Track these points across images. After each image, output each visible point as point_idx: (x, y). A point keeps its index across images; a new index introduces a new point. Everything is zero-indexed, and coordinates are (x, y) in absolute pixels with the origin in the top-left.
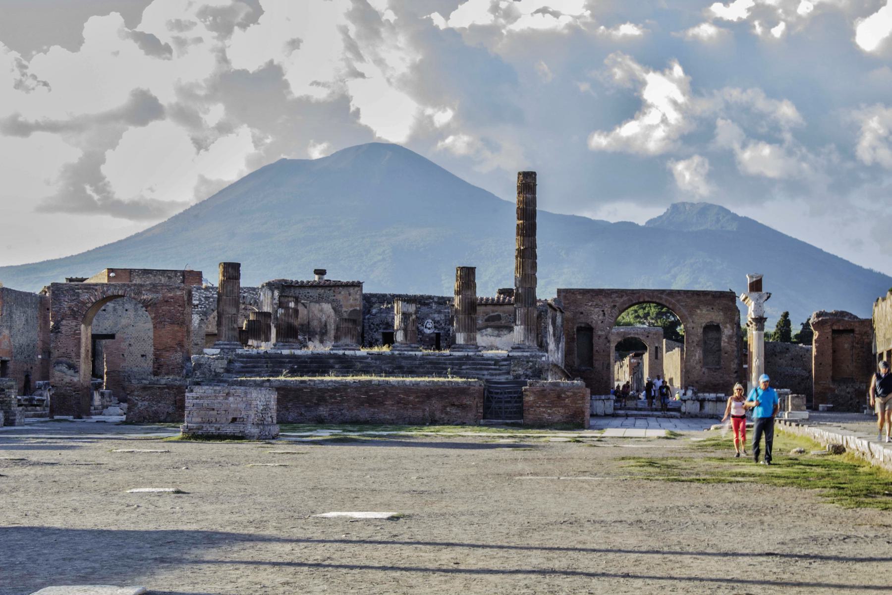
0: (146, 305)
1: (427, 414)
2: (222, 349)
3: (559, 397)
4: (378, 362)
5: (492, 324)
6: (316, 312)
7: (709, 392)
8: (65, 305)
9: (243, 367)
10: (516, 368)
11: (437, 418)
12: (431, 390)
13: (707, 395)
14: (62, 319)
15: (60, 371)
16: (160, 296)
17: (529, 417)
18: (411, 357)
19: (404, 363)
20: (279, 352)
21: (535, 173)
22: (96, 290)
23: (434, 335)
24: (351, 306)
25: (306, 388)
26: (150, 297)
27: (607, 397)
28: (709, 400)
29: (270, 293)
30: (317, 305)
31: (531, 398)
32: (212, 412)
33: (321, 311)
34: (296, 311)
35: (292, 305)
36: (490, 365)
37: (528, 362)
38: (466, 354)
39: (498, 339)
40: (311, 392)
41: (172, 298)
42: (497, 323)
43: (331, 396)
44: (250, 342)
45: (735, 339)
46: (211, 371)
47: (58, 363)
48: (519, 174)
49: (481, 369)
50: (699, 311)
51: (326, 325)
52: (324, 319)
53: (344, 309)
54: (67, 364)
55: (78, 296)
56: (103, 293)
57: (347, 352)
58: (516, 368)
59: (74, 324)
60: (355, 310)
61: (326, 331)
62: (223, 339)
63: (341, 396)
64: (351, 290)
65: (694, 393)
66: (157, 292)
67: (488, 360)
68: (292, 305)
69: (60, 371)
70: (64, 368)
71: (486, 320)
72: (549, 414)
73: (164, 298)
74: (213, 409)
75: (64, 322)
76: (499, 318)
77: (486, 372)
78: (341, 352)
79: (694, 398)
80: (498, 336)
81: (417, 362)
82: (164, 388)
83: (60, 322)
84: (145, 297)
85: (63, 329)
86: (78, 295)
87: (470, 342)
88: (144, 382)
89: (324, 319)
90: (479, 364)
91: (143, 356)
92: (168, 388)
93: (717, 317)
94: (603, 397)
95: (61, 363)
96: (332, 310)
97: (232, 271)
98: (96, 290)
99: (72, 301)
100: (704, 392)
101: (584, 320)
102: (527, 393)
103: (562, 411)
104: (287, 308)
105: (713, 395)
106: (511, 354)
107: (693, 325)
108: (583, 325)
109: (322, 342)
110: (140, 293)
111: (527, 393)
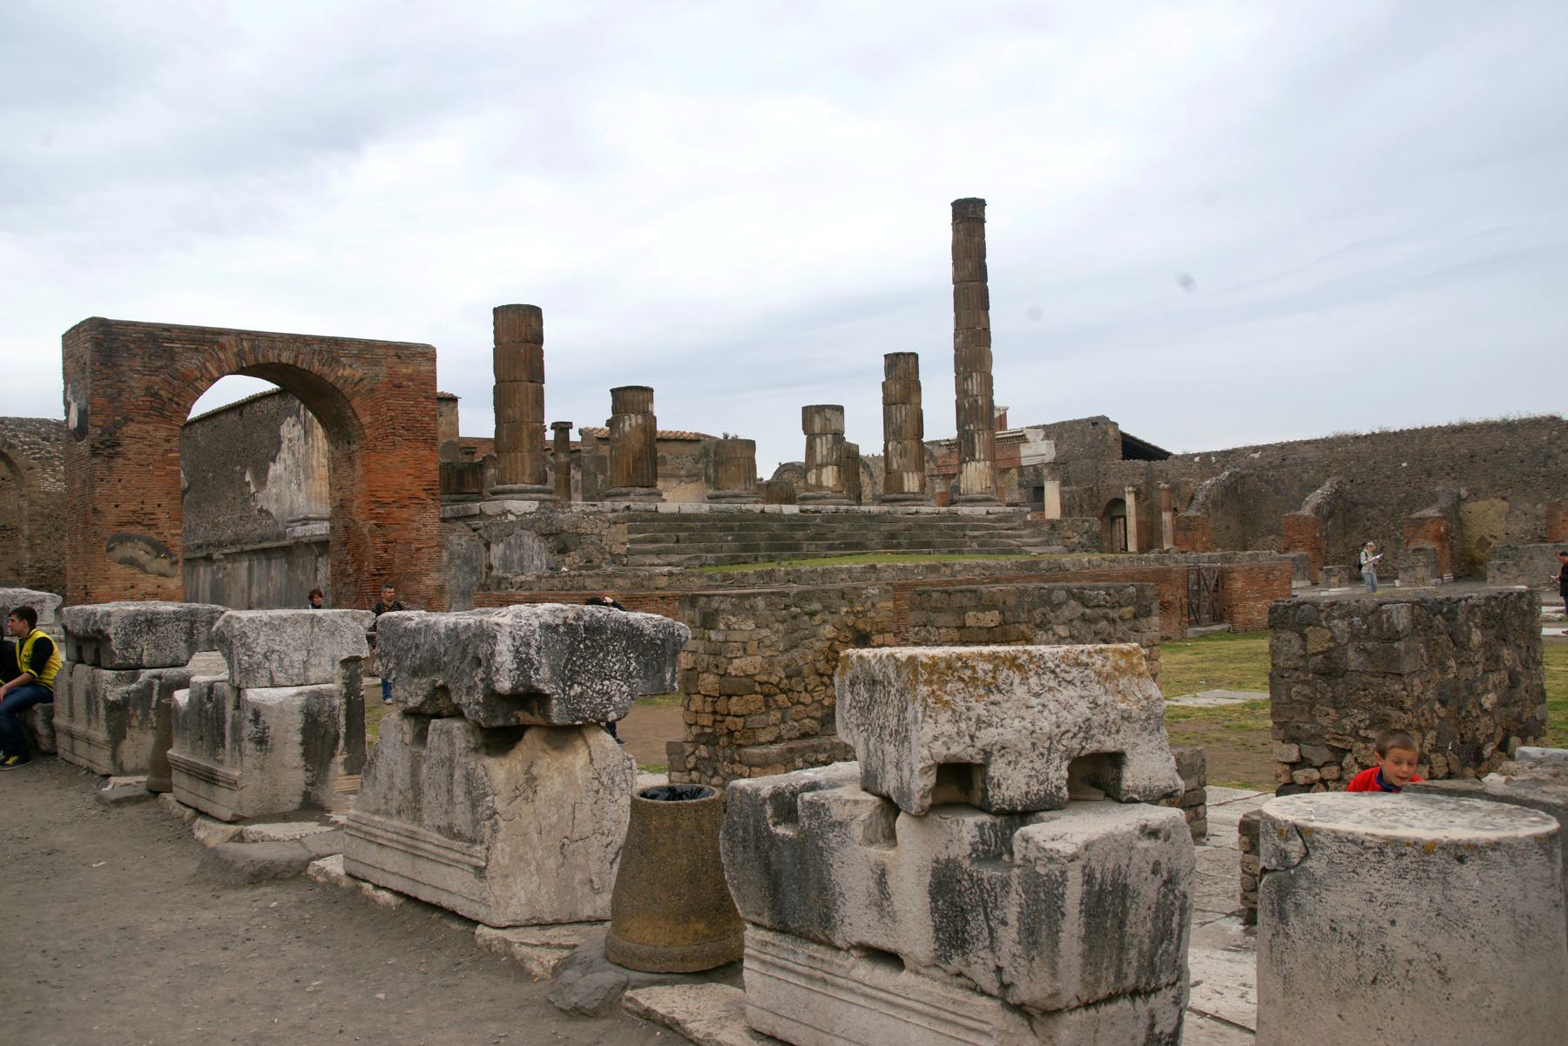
2: (542, 501)
3: (1267, 580)
10: (1069, 534)
14: (128, 420)
15: (131, 562)
16: (383, 371)
22: (222, 347)
26: (359, 374)
41: (410, 378)
46: (602, 551)
47: (123, 539)
54: (149, 542)
55: (172, 359)
59: (163, 434)
69: (131, 562)
70: (140, 552)
75: (132, 429)
83: (118, 426)
84: (348, 372)
85: (130, 447)
88: (619, 582)
95: (129, 538)
98: (222, 347)
99: (154, 371)
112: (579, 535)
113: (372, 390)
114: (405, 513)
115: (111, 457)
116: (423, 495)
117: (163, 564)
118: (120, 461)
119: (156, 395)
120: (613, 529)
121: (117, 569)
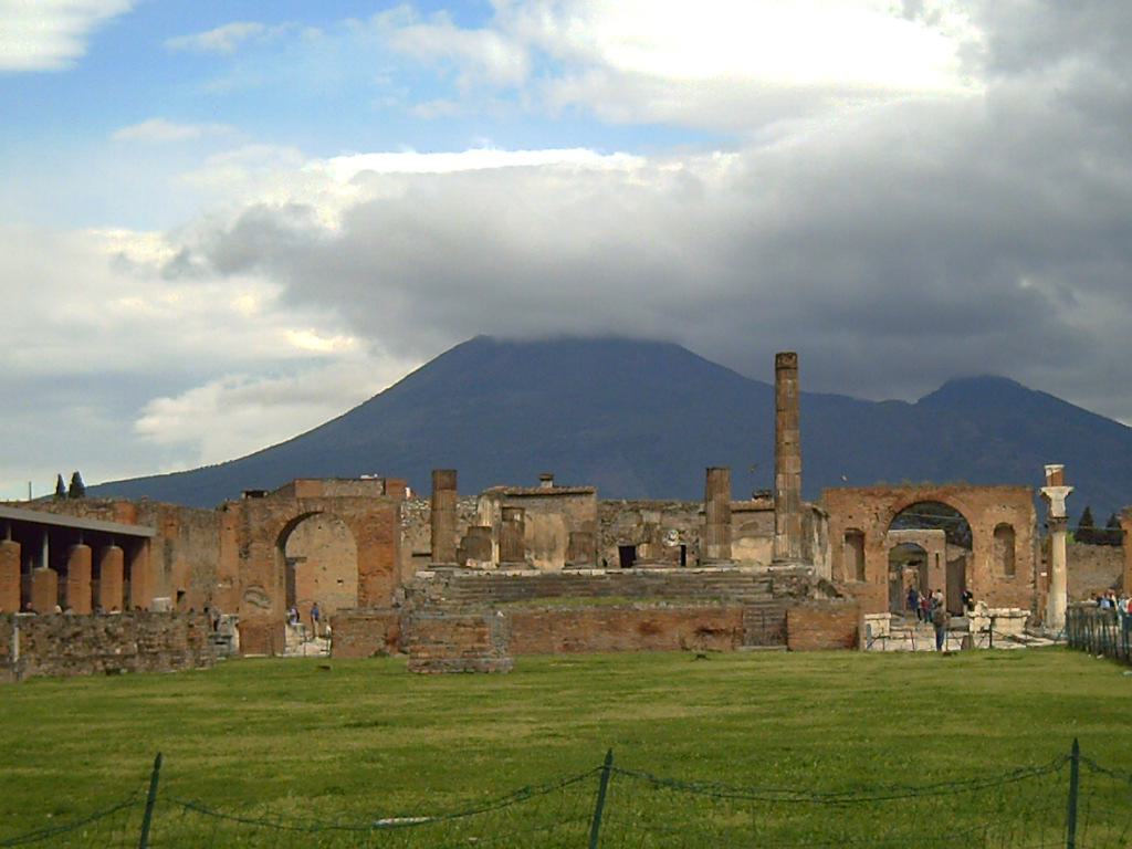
0: (350, 521)
1: (677, 641)
2: (437, 572)
3: (830, 618)
4: (618, 583)
5: (747, 533)
6: (543, 524)
7: (1003, 607)
8: (255, 526)
9: (462, 593)
11: (688, 646)
13: (999, 611)
14: (252, 542)
15: (251, 602)
17: (793, 642)
18: (657, 576)
19: (648, 582)
20: (503, 573)
21: (795, 354)
23: (679, 549)
24: (584, 516)
25: (537, 614)
27: (882, 615)
28: (1002, 617)
29: (489, 504)
30: (544, 517)
31: (797, 620)
32: (440, 646)
33: (549, 523)
34: (522, 525)
35: (518, 517)
36: (748, 582)
37: (792, 577)
38: (720, 570)
39: (755, 551)
40: (542, 619)
41: (378, 513)
42: (754, 532)
43: (565, 623)
44: (468, 564)
45: (1031, 542)
47: (248, 592)
48: (778, 356)
49: (738, 587)
50: (988, 511)
51: (554, 540)
52: (552, 534)
54: (260, 594)
57: (581, 572)
60: (588, 522)
61: (555, 546)
63: (576, 623)
64: (584, 498)
65: (985, 608)
66: (361, 507)
67: (745, 576)
68: (518, 517)
69: (251, 602)
71: (741, 529)
72: (818, 638)
74: (442, 642)
75: (254, 545)
76: (755, 525)
77: (742, 591)
78: (575, 572)
79: (984, 614)
80: (755, 547)
81: (664, 582)
82: (372, 620)
83: (247, 546)
85: (254, 553)
87: (726, 556)
88: (350, 612)
89: (552, 532)
90: (735, 582)
91: (339, 581)
92: (377, 619)
93: (1008, 516)
94: (877, 616)
95: (252, 591)
96: (561, 522)
99: (263, 520)
100: (995, 608)
101: (853, 526)
103: (833, 634)
104: (512, 520)
105: (1006, 611)
106: (772, 569)
107: (982, 528)
109: (550, 559)
110: (341, 508)
112: (413, 591)
113: (360, 521)
114: (375, 578)
115: (246, 558)
117: (265, 603)
118: (249, 560)
120: (432, 587)
121: (248, 605)
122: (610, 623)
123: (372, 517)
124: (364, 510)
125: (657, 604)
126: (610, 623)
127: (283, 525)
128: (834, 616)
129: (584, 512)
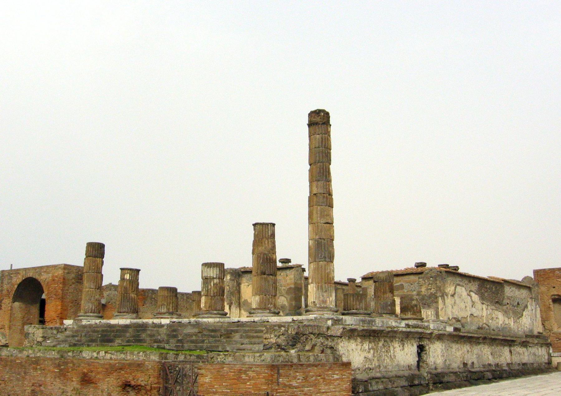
12: (110, 364)
20: (108, 321)
31: (207, 380)
40: (21, 362)
41: (57, 277)
43: (34, 368)
53: (283, 288)
56: (23, 277)
58: (267, 336)
60: (290, 288)
62: (82, 311)
64: (288, 272)
66: (48, 273)
73: (53, 276)
86: (11, 278)
97: (96, 251)
101: (556, 293)
102: (203, 371)
108: (557, 297)
111: (203, 371)
116: (56, 318)
119: (8, 291)
122: (61, 370)
123: (54, 280)
124: (50, 275)
125: (98, 353)
126: (61, 370)
127: (16, 286)
128: (244, 376)
129: (288, 281)
